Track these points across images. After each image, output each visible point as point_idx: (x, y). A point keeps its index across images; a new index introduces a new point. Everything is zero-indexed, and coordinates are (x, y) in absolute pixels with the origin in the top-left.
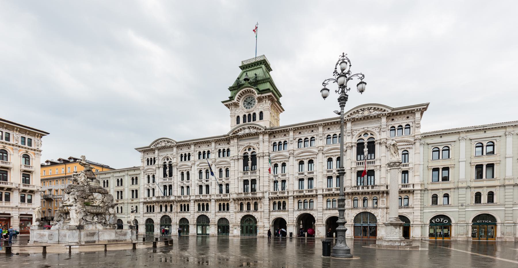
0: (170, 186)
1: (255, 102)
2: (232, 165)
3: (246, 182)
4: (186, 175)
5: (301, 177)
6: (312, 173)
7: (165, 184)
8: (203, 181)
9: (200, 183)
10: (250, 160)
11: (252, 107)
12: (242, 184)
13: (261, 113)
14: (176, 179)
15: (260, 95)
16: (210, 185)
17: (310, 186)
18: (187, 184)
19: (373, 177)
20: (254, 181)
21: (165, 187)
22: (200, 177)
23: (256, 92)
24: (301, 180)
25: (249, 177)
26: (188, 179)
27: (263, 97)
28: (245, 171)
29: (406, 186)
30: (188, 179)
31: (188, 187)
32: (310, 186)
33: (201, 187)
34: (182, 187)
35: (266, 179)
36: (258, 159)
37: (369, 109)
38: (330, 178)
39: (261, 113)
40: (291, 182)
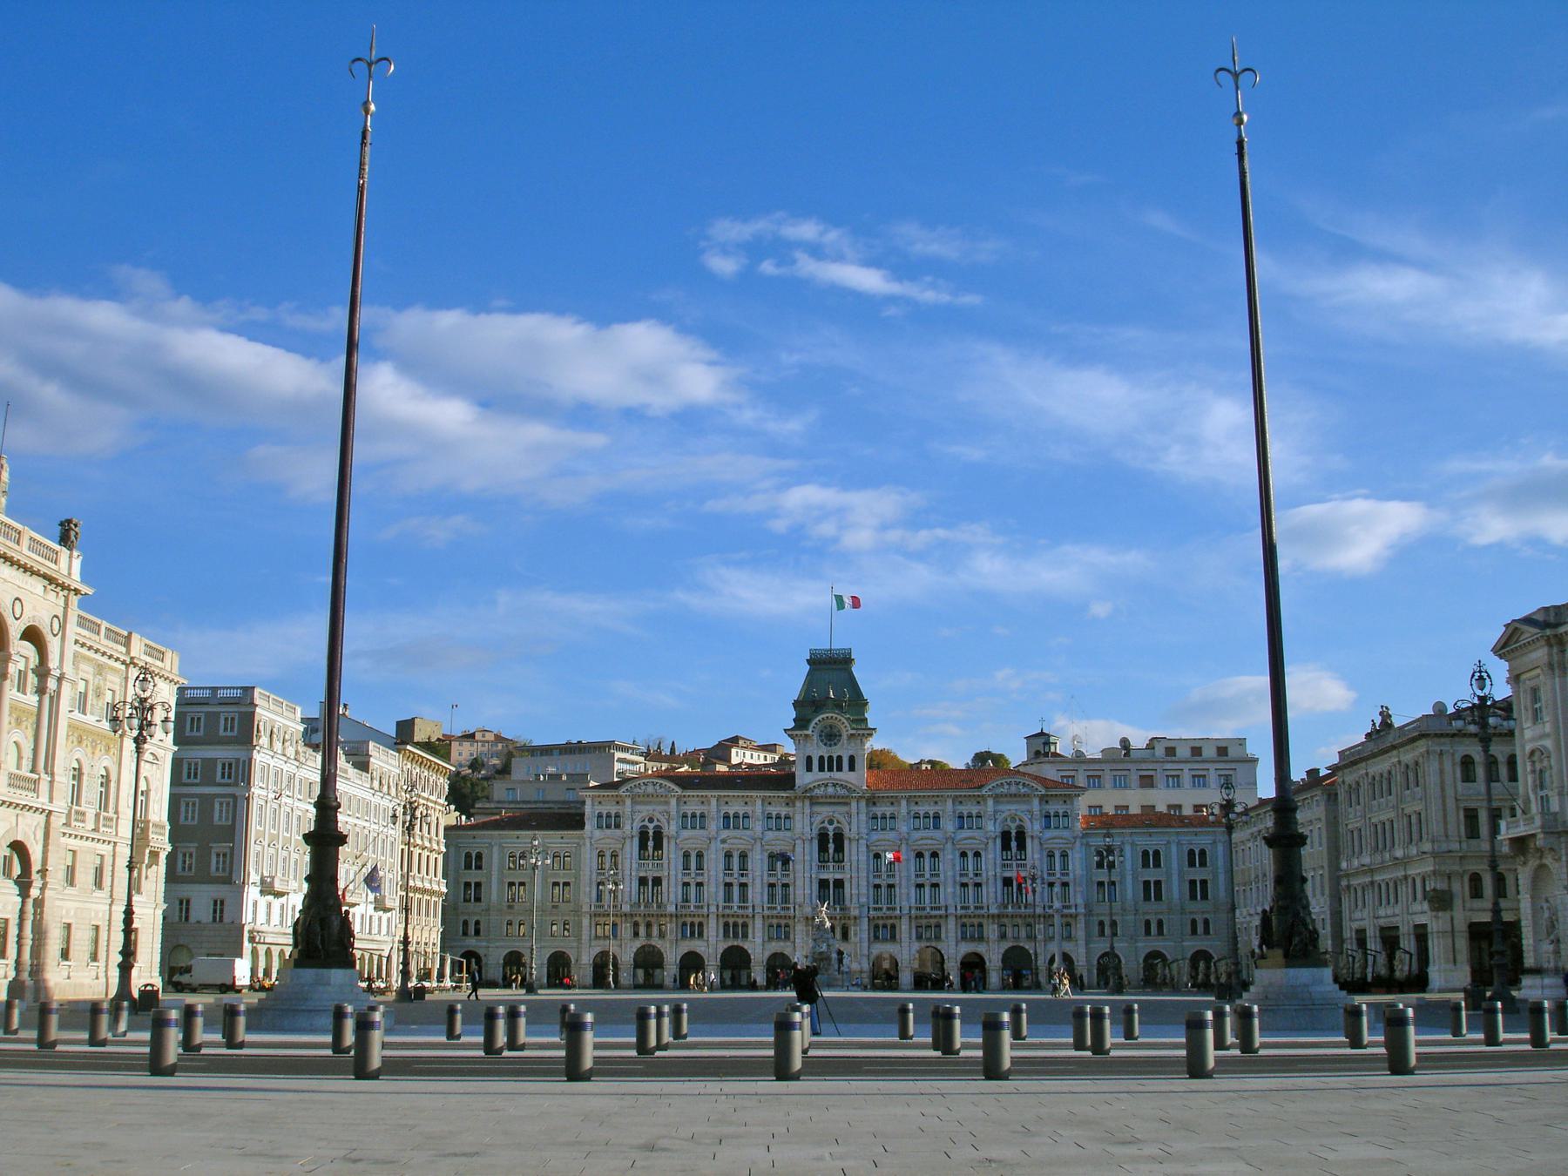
0: (657, 881)
2: (799, 849)
4: (694, 860)
5: (920, 881)
7: (642, 874)
10: (830, 844)
12: (815, 887)
14: (670, 865)
17: (934, 898)
20: (839, 884)
21: (643, 881)
25: (830, 875)
26: (700, 867)
28: (823, 861)
29: (1069, 907)
30: (700, 867)
33: (728, 885)
35: (863, 883)
36: (846, 843)
40: (904, 891)
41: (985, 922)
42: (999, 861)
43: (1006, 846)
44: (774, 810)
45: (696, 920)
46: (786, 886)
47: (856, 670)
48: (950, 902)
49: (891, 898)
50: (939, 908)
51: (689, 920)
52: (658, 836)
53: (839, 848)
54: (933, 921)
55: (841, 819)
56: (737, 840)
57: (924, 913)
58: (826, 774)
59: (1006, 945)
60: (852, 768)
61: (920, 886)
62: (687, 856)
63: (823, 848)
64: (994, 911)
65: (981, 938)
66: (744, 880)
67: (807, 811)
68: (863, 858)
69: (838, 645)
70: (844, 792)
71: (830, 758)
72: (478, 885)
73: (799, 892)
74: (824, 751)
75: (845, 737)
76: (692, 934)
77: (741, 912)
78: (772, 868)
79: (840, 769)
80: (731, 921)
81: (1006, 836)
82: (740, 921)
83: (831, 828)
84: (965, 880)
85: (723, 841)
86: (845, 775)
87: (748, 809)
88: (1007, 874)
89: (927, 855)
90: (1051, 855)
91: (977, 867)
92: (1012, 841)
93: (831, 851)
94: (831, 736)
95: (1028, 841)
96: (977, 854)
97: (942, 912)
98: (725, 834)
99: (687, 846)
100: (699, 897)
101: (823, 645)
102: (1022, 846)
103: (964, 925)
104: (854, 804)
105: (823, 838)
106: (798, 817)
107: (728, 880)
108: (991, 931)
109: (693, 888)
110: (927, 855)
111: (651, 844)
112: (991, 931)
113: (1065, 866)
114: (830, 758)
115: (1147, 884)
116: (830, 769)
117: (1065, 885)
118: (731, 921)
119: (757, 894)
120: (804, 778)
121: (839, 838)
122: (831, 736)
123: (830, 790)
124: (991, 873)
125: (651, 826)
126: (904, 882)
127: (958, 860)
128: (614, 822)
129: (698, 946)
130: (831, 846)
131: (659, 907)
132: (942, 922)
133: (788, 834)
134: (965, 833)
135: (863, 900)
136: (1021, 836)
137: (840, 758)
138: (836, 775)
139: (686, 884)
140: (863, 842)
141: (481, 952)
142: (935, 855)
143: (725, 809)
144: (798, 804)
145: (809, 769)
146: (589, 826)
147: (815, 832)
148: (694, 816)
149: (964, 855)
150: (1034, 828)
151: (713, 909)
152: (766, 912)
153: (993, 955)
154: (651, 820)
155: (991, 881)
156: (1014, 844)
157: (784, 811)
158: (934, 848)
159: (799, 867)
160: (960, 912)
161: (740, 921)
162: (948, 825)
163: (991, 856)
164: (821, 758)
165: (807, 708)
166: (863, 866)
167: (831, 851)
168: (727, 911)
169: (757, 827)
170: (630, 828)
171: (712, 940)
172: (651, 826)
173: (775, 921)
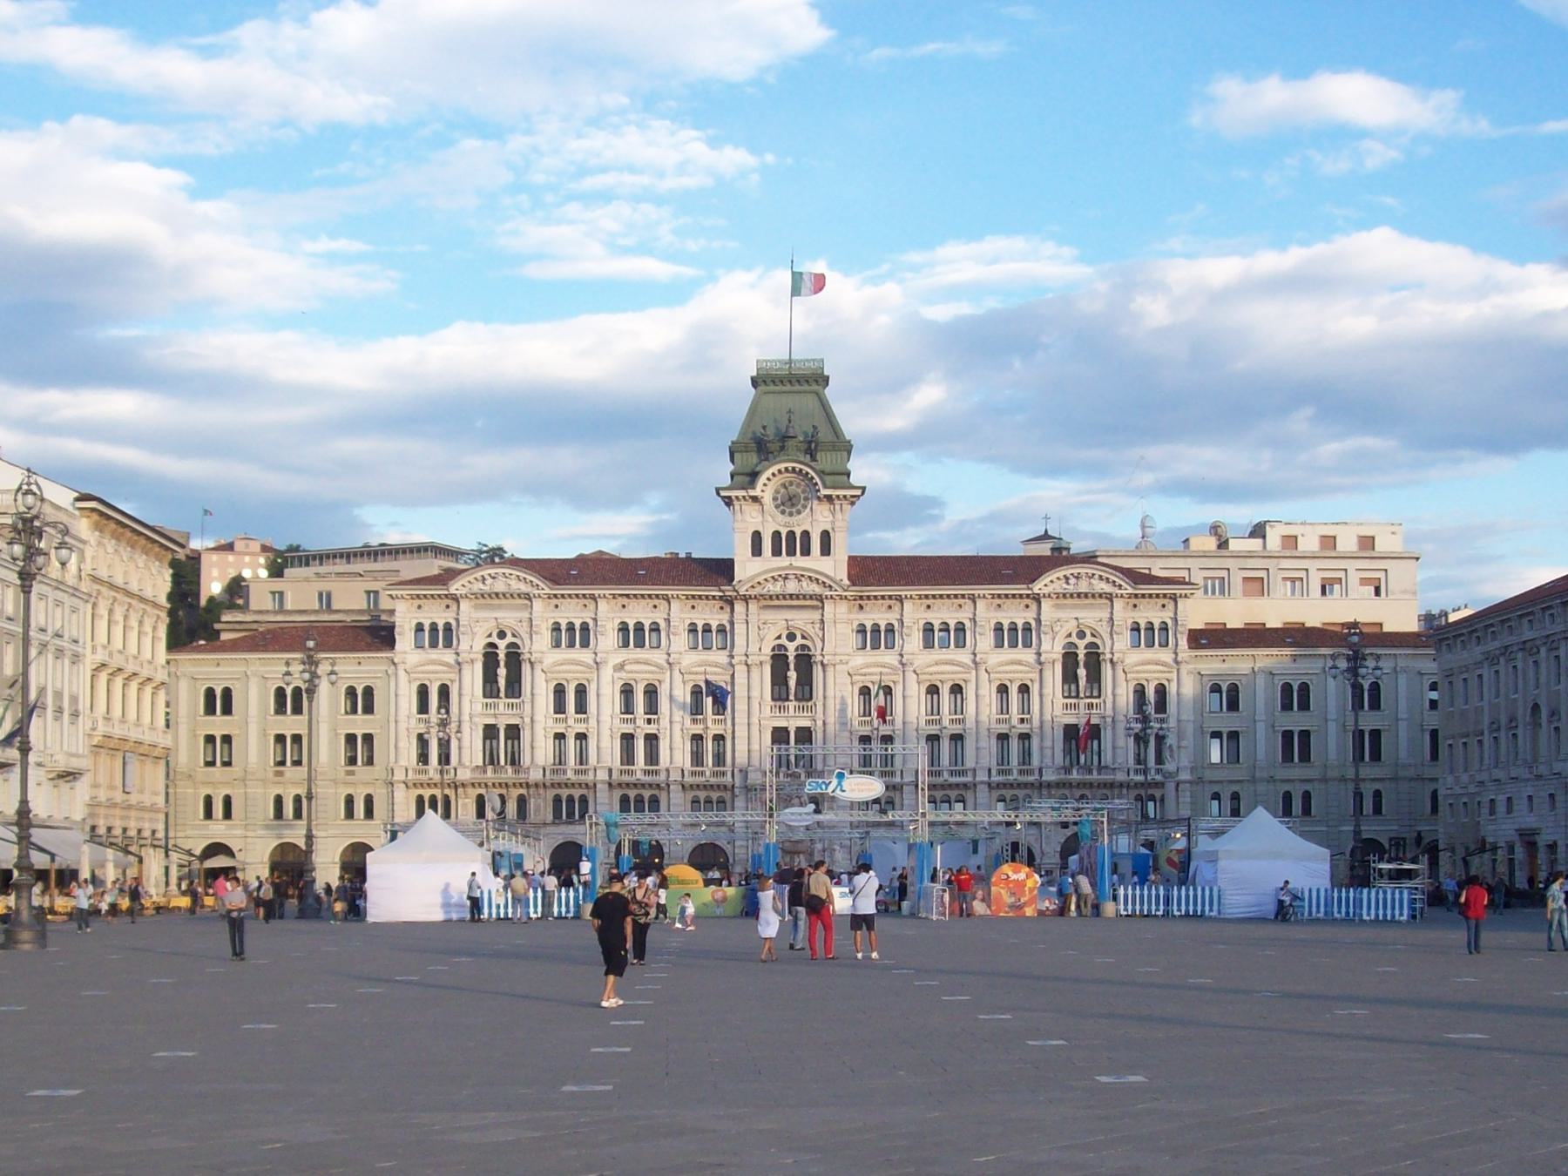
0: (514, 732)
3: (780, 735)
4: (572, 698)
7: (491, 721)
8: (640, 722)
9: (628, 729)
11: (799, 512)
19: (1096, 743)
21: (490, 732)
22: (628, 708)
23: (817, 479)
25: (793, 719)
31: (581, 737)
33: (628, 739)
34: (560, 737)
39: (826, 537)
43: (1070, 676)
45: (577, 793)
46: (719, 738)
47: (829, 393)
50: (963, 773)
51: (565, 793)
52: (514, 658)
53: (806, 681)
54: (953, 794)
55: (809, 630)
56: (643, 665)
57: (940, 780)
58: (784, 561)
60: (826, 550)
63: (779, 679)
64: (1049, 777)
70: (810, 588)
71: (791, 534)
72: (227, 739)
73: (741, 747)
76: (570, 814)
77: (648, 779)
78: (696, 709)
79: (806, 551)
80: (632, 794)
82: (647, 794)
83: (791, 647)
85: (620, 667)
86: (815, 562)
89: (945, 691)
91: (1025, 708)
93: (792, 683)
95: (1107, 671)
97: (969, 779)
98: (623, 655)
100: (582, 758)
102: (1095, 677)
104: (828, 606)
105: (779, 660)
106: (740, 629)
109: (571, 742)
110: (945, 691)
111: (502, 672)
114: (791, 534)
115: (1287, 736)
116: (791, 552)
118: (632, 794)
120: (747, 569)
121: (805, 662)
123: (792, 587)
125: (502, 644)
128: (443, 636)
130: (792, 676)
131: (516, 772)
137: (806, 534)
138: (799, 561)
141: (234, 845)
142: (957, 689)
144: (739, 607)
145: (757, 550)
146: (405, 639)
147: (767, 651)
154: (502, 635)
156: (1082, 672)
158: (958, 679)
159: (741, 706)
160: (996, 778)
161: (647, 794)
164: (776, 535)
167: (792, 683)
168: (626, 778)
170: (472, 644)
172: (502, 644)
173: (702, 795)
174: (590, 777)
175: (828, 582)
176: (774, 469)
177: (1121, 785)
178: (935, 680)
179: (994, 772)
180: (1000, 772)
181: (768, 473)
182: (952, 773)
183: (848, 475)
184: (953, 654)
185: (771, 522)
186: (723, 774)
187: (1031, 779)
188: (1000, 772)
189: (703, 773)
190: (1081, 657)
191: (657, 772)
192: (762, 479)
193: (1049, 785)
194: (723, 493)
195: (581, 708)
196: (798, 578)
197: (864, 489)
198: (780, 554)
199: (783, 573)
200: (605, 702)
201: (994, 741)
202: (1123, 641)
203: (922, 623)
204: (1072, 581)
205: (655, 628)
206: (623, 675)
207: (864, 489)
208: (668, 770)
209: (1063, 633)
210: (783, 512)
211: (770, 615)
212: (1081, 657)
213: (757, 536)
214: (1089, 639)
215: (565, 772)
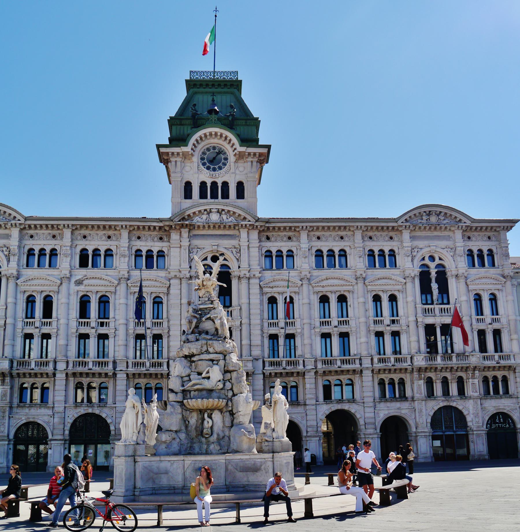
1: (226, 159)
2: (174, 291)
5: (326, 329)
6: (347, 322)
8: (93, 324)
11: (220, 168)
13: (240, 186)
15: (243, 149)
16: (111, 336)
17: (345, 349)
18: (46, 330)
22: (84, 312)
24: (326, 336)
27: (249, 154)
29: (508, 357)
32: (345, 349)
35: (256, 332)
36: (234, 283)
37: (439, 214)
38: (379, 335)
41: (407, 378)
42: (420, 306)
43: (426, 289)
44: (144, 246)
46: (157, 338)
48: (364, 353)
49: (291, 349)
54: (344, 378)
56: (96, 281)
58: (209, 200)
59: (434, 405)
60: (240, 195)
61: (326, 336)
62: (30, 301)
64: (420, 361)
65: (403, 397)
66: (103, 330)
67: (185, 243)
68: (255, 300)
69: (224, 65)
71: (214, 184)
74: (207, 177)
75: (232, 158)
77: (97, 369)
81: (424, 277)
84: (380, 328)
85: (79, 283)
87: (111, 244)
88: (430, 320)
90: (478, 299)
92: (433, 283)
94: (214, 160)
95: (452, 284)
96: (393, 298)
97: (357, 366)
99: (30, 289)
101: (204, 66)
102: (444, 289)
103: (382, 383)
107: (84, 330)
108: (416, 387)
112: (416, 387)
113: (495, 311)
114: (214, 184)
116: (214, 196)
117: (497, 333)
119: (120, 348)
122: (214, 160)
123: (215, 217)
124: (412, 319)
126: (306, 327)
127: (371, 304)
129: (40, 415)
132: (357, 379)
133: (162, 273)
134: (379, 272)
135: (256, 352)
136: (442, 278)
137: (225, 184)
139: (29, 336)
140: (254, 282)
142: (342, 299)
143: (81, 244)
144: (174, 236)
148: (42, 251)
149: (377, 299)
150: (456, 265)
151: (61, 366)
152: (131, 370)
153: (419, 414)
155: (412, 326)
156: (435, 286)
157: (156, 247)
158: (342, 290)
159: (174, 312)
160: (378, 366)
162: (357, 261)
163: (410, 299)
164: (203, 184)
165: (184, 124)
166: (256, 310)
168: (80, 369)
169: (122, 263)
171: (59, 407)
174: (50, 368)
175: (243, 214)
176: (201, 133)
177: (475, 368)
178: (325, 290)
179: (376, 360)
180: (380, 361)
181: (196, 136)
182: (343, 362)
183: (257, 140)
184: (337, 272)
185: (198, 175)
186: (160, 365)
187: (405, 365)
188: (380, 361)
189: (143, 364)
190: (433, 275)
191: (106, 364)
192: (192, 140)
193: (420, 370)
194: (162, 150)
195: (48, 312)
196: (220, 212)
197: (269, 147)
198: (206, 198)
199: (208, 207)
200: (66, 310)
201: (373, 338)
202: (463, 263)
203: (314, 250)
204: (425, 218)
205: (109, 253)
206: (81, 288)
207: (269, 147)
208: (114, 362)
209: (419, 257)
210: (208, 168)
211: (197, 242)
212: (433, 275)
213: (188, 186)
214: (437, 261)
215: (29, 364)
